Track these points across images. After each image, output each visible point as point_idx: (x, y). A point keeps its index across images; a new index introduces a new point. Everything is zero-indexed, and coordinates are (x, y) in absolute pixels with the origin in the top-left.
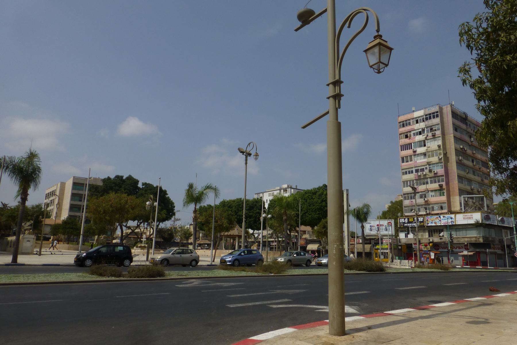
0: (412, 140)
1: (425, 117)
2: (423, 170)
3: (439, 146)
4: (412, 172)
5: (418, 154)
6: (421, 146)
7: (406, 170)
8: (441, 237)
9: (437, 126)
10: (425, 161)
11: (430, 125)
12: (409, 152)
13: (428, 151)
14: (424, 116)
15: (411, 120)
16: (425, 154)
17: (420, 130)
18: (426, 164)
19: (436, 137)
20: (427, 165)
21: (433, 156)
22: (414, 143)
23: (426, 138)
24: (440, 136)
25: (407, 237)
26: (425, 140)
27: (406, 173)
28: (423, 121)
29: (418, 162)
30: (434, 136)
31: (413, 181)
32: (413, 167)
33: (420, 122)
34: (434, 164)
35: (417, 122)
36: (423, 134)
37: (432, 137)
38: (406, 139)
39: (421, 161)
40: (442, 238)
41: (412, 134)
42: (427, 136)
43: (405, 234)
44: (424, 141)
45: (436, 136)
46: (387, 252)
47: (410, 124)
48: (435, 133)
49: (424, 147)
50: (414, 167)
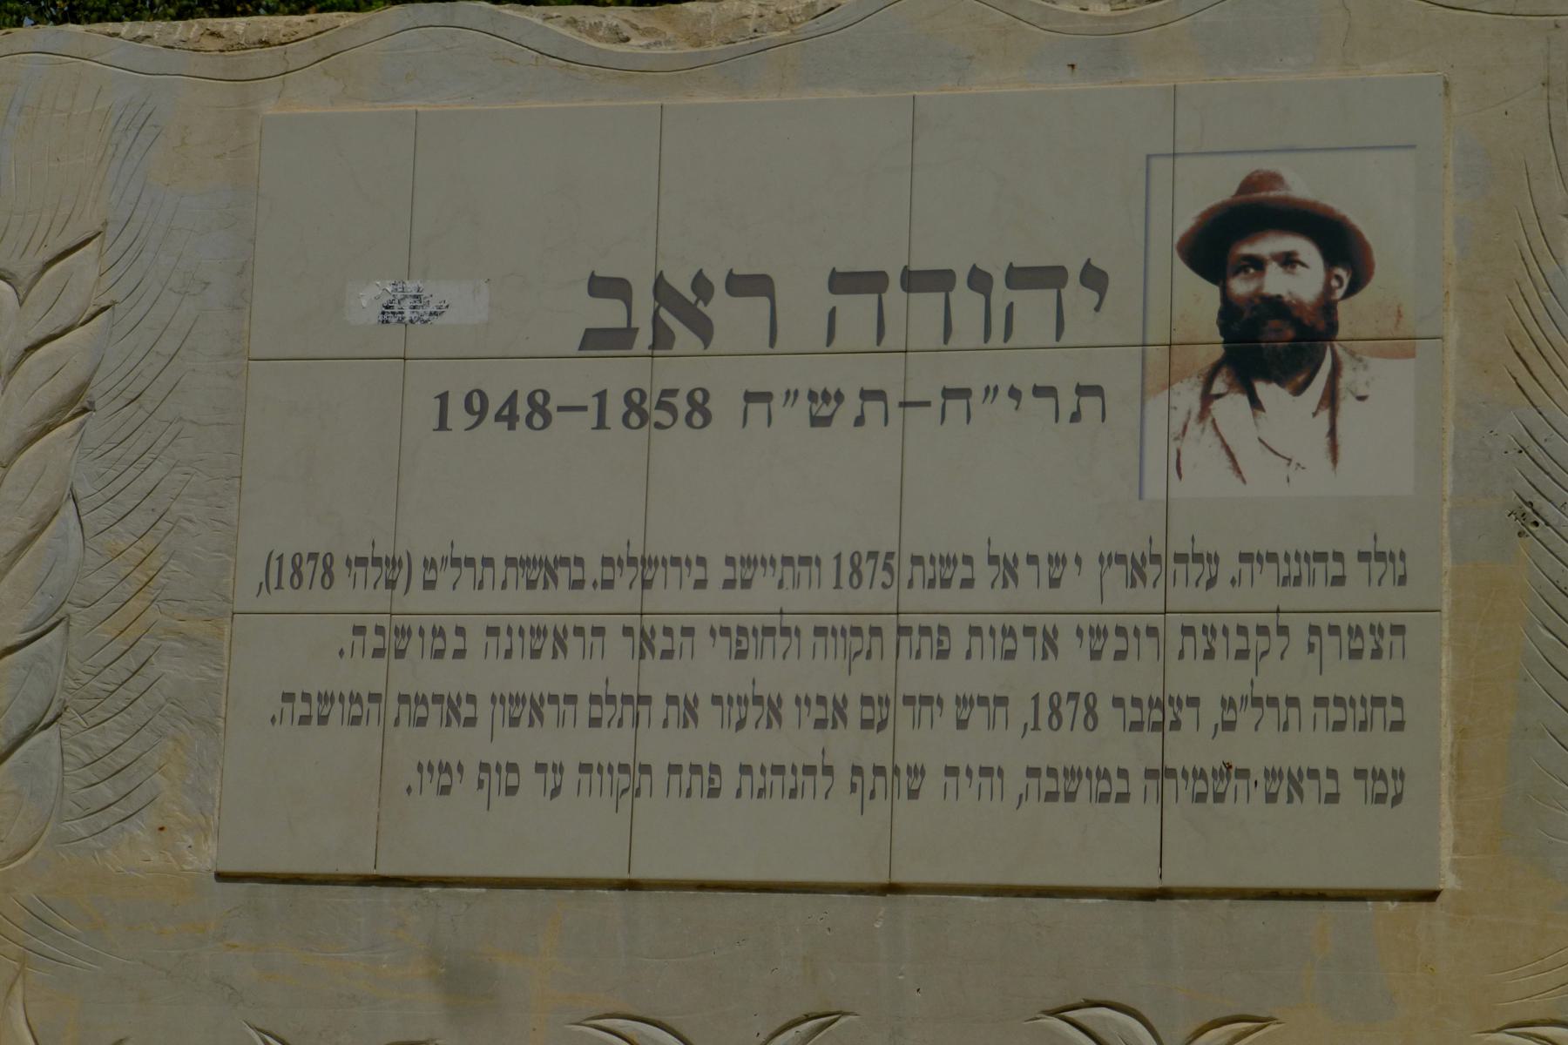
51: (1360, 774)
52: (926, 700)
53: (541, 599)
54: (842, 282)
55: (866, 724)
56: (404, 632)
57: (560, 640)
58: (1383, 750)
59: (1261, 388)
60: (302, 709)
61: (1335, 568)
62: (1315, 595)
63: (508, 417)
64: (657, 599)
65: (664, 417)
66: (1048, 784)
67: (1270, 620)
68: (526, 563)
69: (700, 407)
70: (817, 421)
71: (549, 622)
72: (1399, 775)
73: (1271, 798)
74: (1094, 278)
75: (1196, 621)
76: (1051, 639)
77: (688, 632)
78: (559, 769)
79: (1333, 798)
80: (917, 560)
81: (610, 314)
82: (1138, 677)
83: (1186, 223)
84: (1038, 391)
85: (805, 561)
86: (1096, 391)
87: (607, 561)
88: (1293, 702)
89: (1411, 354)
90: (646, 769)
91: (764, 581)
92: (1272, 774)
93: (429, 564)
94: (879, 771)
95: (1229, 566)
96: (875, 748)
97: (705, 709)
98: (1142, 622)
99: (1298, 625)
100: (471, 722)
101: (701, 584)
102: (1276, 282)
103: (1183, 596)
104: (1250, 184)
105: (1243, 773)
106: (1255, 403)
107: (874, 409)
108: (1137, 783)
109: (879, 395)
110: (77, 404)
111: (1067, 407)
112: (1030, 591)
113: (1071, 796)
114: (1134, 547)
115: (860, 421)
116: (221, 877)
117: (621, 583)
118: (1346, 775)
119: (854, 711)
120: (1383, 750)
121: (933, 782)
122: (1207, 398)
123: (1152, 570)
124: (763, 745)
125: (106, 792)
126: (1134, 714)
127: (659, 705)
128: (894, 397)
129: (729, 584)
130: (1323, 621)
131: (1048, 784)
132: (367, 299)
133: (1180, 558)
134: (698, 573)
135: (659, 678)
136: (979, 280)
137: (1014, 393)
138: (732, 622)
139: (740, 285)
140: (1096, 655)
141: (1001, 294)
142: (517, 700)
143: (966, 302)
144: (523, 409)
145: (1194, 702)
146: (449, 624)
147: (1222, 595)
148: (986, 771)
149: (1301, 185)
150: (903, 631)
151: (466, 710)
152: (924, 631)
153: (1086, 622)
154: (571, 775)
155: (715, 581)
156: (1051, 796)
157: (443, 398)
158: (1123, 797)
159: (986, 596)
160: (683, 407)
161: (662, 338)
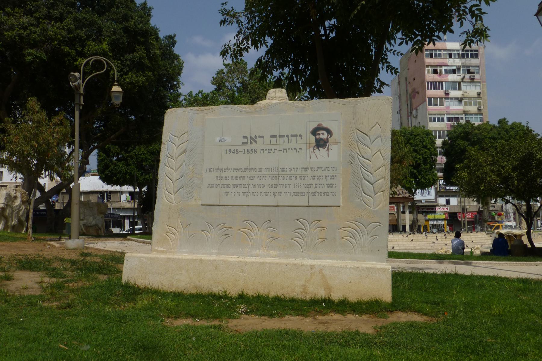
0: (443, 78)
1: (460, 53)
2: (457, 119)
3: (479, 94)
4: (443, 120)
5: (452, 98)
6: (454, 89)
7: (434, 116)
8: (493, 205)
9: (476, 68)
10: (460, 109)
11: (468, 65)
12: (439, 93)
13: (465, 96)
14: (460, 51)
15: (442, 51)
16: (460, 100)
17: (455, 68)
18: (462, 113)
19: (475, 82)
20: (463, 114)
21: (470, 104)
22: (445, 82)
23: (462, 79)
24: (480, 82)
25: (449, 204)
26: (461, 82)
27: (435, 121)
28: (459, 57)
29: (451, 108)
30: (472, 80)
31: (444, 131)
32: (444, 114)
33: (455, 57)
34: (472, 114)
35: (450, 56)
36: (458, 73)
37: (470, 81)
38: (435, 75)
39: (455, 107)
40: (494, 206)
41: (443, 71)
42: (464, 77)
43: (447, 200)
44: (459, 83)
45: (475, 81)
46: (443, 224)
47: (440, 55)
48: (474, 76)
49: (460, 91)
50: (447, 114)
51: (331, 192)
52: (282, 185)
53: (237, 173)
54: (272, 136)
55: (275, 187)
56: (222, 177)
57: (240, 178)
58: (333, 190)
59: (320, 148)
60: (211, 186)
61: (328, 169)
62: (326, 172)
63: (234, 152)
64: (251, 173)
65: (251, 152)
66: (296, 194)
67: (321, 175)
68: (236, 169)
69: (256, 151)
70: (269, 152)
71: (238, 176)
72: (336, 193)
73: (321, 195)
74: (301, 136)
75: (313, 175)
76: (296, 177)
77: (254, 177)
78: (240, 193)
79: (328, 195)
80: (281, 168)
81: (245, 140)
82: (306, 182)
83: (311, 129)
84: (294, 149)
85: (268, 169)
86: (301, 149)
87: (245, 169)
88: (323, 184)
89: (337, 144)
90: (250, 193)
91: (263, 171)
92: (321, 193)
93: (225, 169)
94: (276, 193)
95: (316, 169)
96: (276, 190)
97: (256, 186)
98: (306, 175)
99: (324, 176)
100: (230, 187)
101: (256, 171)
102: (322, 136)
103: (311, 172)
104: (319, 125)
105: (318, 193)
106: (319, 150)
107: (276, 151)
108: (306, 194)
109: (276, 149)
110: (185, 151)
111: (298, 151)
112: (294, 172)
113: (298, 195)
114: (305, 167)
115: (274, 152)
116: (202, 205)
117: (247, 171)
118: (330, 193)
119: (273, 186)
120: (333, 190)
121: (282, 194)
122: (314, 150)
123: (307, 169)
124: (263, 190)
125: (189, 195)
126: (305, 186)
127: (251, 186)
128: (278, 150)
129: (259, 171)
130: (327, 175)
131: (296, 194)
132: (218, 139)
133: (311, 168)
134: (255, 170)
135: (251, 182)
136: (288, 136)
137: (292, 149)
138: (259, 176)
139: (260, 137)
140: (301, 179)
141: (290, 138)
142: (235, 185)
143: (286, 139)
144: (235, 151)
145: (312, 184)
146: (227, 176)
147: (316, 172)
148: (288, 193)
149: (324, 125)
150: (279, 177)
151: (229, 186)
152: (282, 177)
153: (300, 175)
154: (241, 193)
155: (257, 171)
156: (296, 195)
157: (226, 150)
158: (304, 195)
159: (289, 172)
160: (254, 151)
161: (251, 143)
